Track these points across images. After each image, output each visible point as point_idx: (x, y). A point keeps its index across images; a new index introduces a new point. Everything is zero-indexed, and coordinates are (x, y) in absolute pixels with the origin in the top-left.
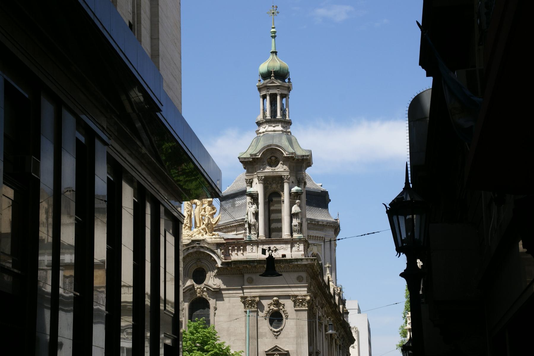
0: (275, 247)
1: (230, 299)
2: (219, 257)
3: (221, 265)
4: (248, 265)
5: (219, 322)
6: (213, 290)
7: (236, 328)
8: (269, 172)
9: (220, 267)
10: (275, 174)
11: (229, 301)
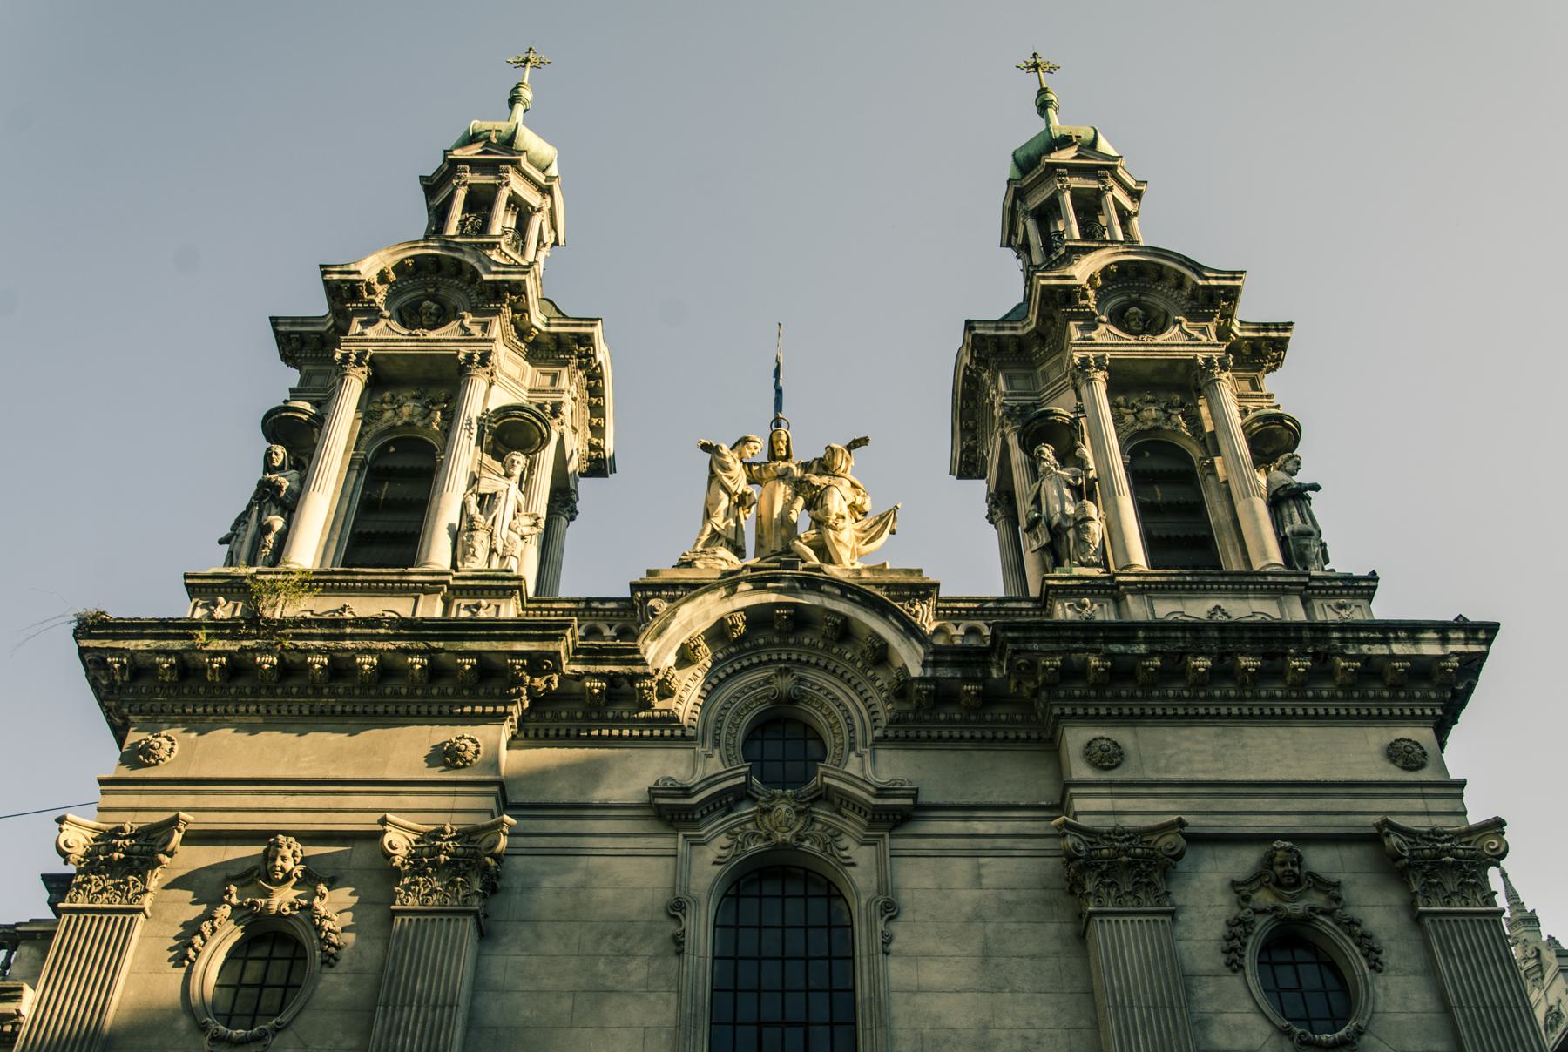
0: (1218, 607)
1: (980, 866)
2: (911, 630)
3: (924, 665)
4: (1096, 652)
5: (920, 990)
6: (874, 801)
7: (1032, 1034)
8: (1127, 345)
9: (921, 680)
10: (1157, 354)
11: (979, 877)
